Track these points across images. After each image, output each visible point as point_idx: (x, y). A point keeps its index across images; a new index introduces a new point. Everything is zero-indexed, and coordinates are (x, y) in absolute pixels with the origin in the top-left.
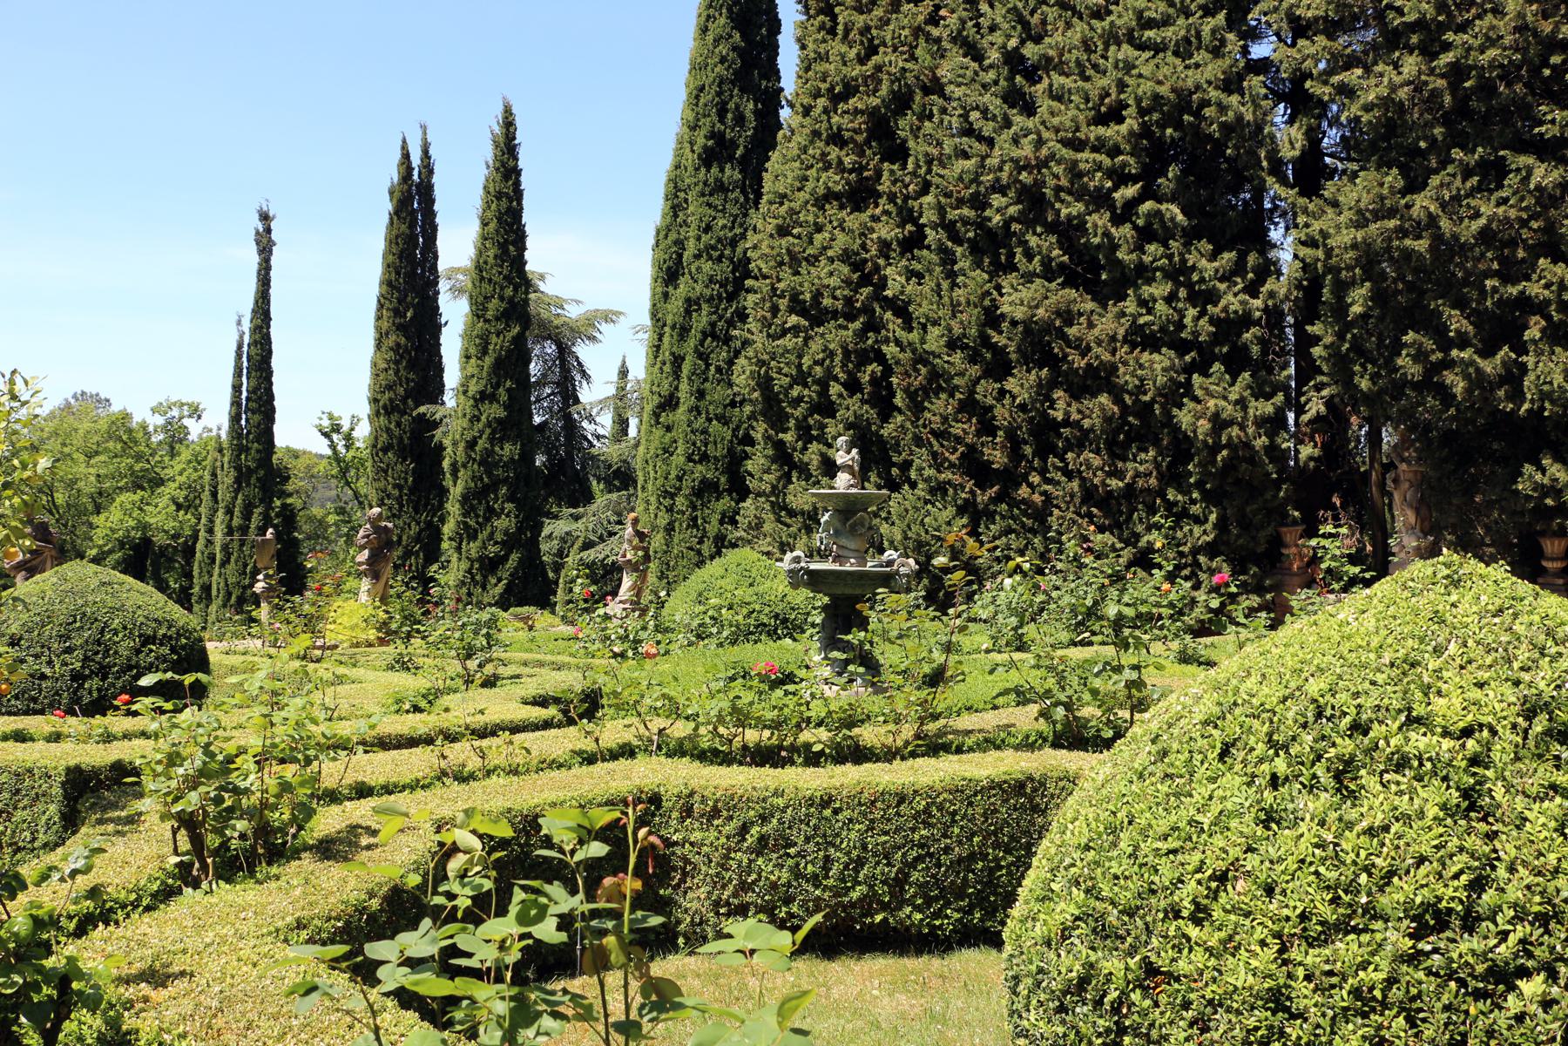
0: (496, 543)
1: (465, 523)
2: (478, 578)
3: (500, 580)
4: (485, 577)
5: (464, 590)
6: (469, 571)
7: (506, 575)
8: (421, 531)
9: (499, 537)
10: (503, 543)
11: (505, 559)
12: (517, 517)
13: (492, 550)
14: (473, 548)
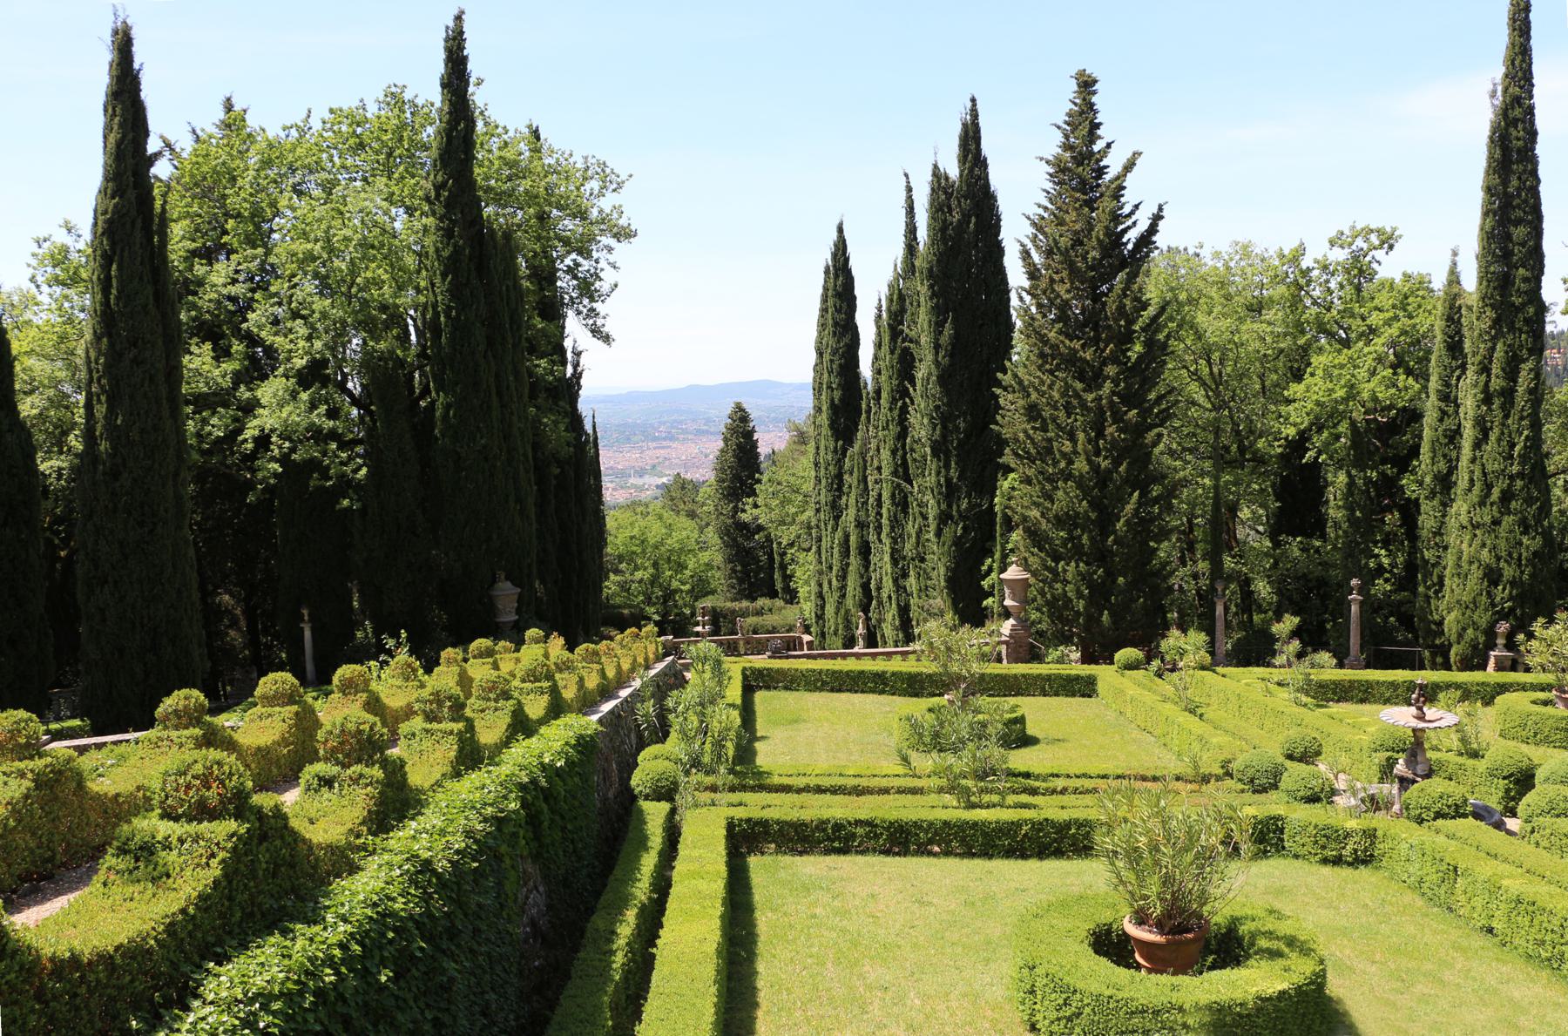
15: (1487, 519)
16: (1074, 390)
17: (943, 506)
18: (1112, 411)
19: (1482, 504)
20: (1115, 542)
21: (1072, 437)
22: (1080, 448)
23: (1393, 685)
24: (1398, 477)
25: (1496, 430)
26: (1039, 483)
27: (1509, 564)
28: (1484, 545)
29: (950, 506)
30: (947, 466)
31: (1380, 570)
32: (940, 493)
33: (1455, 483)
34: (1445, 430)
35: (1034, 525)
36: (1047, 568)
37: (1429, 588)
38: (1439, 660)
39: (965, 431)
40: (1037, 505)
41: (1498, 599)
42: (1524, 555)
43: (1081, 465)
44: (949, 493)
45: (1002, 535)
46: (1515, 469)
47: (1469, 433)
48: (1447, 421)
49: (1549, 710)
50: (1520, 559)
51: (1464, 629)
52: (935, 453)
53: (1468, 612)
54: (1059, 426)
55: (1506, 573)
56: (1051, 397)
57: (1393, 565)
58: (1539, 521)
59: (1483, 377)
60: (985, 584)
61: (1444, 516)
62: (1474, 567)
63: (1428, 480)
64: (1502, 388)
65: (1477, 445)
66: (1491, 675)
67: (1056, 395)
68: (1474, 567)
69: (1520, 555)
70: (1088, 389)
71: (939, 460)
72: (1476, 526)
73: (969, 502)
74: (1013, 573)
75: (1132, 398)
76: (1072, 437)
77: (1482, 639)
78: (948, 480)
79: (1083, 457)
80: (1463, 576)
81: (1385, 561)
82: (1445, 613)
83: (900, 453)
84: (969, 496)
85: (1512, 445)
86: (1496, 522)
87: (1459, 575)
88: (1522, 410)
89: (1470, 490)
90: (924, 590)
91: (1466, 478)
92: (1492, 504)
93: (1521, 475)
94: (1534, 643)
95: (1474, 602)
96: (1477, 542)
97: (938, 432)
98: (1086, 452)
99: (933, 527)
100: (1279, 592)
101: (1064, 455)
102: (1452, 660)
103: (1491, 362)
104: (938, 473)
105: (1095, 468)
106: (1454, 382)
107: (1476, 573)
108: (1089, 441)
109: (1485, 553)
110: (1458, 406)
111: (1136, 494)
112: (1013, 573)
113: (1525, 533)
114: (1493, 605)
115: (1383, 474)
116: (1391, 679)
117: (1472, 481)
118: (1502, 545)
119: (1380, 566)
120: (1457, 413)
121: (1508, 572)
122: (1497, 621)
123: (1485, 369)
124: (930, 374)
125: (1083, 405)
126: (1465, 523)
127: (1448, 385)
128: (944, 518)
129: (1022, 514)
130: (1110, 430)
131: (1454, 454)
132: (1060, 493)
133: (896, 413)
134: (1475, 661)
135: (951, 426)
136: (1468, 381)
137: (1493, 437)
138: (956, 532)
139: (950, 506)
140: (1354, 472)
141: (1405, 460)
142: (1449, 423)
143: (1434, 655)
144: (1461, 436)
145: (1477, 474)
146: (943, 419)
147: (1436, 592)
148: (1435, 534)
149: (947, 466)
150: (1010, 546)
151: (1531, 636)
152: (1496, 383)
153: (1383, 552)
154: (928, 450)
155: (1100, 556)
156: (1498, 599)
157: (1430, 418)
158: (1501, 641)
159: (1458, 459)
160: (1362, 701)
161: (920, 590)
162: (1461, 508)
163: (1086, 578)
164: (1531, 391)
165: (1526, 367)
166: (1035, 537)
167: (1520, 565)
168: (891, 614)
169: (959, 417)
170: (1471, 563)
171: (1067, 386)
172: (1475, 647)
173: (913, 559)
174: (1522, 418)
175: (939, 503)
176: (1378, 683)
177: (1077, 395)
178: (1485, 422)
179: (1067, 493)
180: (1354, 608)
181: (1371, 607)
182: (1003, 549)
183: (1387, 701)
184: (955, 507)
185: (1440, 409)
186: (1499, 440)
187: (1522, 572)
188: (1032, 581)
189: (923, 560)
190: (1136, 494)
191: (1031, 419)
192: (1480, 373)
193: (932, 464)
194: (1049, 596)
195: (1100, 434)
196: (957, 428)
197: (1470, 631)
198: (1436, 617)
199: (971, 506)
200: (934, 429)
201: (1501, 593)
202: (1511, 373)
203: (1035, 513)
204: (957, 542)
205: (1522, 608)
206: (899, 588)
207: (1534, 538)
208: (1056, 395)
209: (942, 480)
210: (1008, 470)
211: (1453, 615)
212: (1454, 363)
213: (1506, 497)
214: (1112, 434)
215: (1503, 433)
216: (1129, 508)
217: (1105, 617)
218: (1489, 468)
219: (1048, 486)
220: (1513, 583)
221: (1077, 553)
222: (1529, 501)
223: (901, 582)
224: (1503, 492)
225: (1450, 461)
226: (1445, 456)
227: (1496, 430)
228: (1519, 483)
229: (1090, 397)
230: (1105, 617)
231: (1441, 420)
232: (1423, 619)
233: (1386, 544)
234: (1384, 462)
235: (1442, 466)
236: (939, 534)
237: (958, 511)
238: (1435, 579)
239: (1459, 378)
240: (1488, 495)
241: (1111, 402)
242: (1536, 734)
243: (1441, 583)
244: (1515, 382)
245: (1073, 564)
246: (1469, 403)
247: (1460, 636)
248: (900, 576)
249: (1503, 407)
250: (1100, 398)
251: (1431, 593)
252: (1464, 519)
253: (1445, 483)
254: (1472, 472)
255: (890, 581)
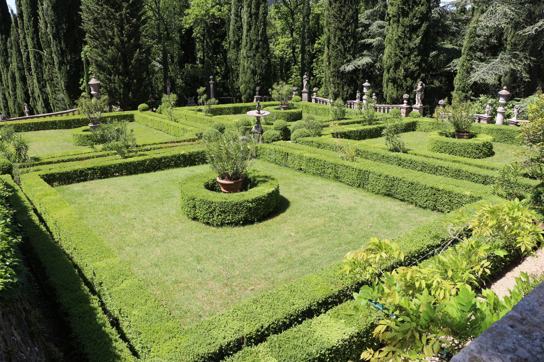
0: (417, 19)
1: (403, 8)
2: (408, 35)
3: (418, 36)
4: (411, 35)
5: (401, 41)
6: (404, 32)
7: (421, 34)
8: (354, 13)
9: (418, 15)
10: (420, 18)
11: (419, 26)
12: (426, 6)
13: (415, 22)
14: (406, 21)
15: (252, 55)
16: (111, 12)
17: (60, 59)
18: (127, 20)
19: (250, 50)
20: (132, 67)
21: (112, 29)
22: (115, 33)
23: (229, 108)
24: (221, 42)
25: (254, 26)
26: (101, 47)
27: (259, 69)
28: (251, 63)
29: (63, 58)
30: (60, 43)
31: (217, 73)
32: (58, 54)
33: (241, 44)
34: (237, 26)
35: (100, 63)
36: (107, 79)
37: (234, 78)
38: (238, 100)
39: (66, 29)
40: (101, 56)
41: (256, 80)
42: (263, 65)
43: (117, 40)
44: (62, 53)
45: (86, 68)
46: (260, 38)
47: (245, 27)
48: (237, 23)
49: (279, 111)
50: (262, 67)
51: (246, 90)
52: (54, 38)
53: (248, 84)
54: (106, 26)
55: (258, 71)
56: (102, 15)
57: (221, 71)
58: (267, 55)
59: (249, 9)
60: (81, 88)
61: (238, 54)
62: (249, 70)
63: (232, 43)
64: (255, 12)
65: (248, 31)
66: (255, 103)
67: (104, 13)
68: (249, 70)
69: (262, 65)
70: (117, 12)
71: (56, 40)
72: (248, 57)
73: (71, 57)
74: (93, 81)
75: (132, 15)
76: (112, 29)
77: (252, 92)
78: (61, 49)
79: (117, 37)
80: (245, 73)
81: (219, 70)
82: (240, 85)
83: (35, 39)
84: (70, 54)
85: (258, 31)
86: (255, 56)
87: (244, 73)
88: (261, 20)
89: (246, 46)
90: (54, 92)
91: (245, 41)
92: (253, 50)
93: (261, 40)
94: (274, 91)
95: (249, 81)
96: (249, 62)
97: (54, 30)
98: (118, 35)
99: (57, 67)
100: (185, 82)
101: (110, 36)
102: (243, 100)
103: (251, 4)
104: (57, 46)
105: (122, 41)
106: (239, 10)
107: (249, 71)
108: (119, 31)
109: (252, 66)
110: (241, 18)
111: (138, 50)
112: (93, 81)
113: (263, 59)
114: (255, 82)
115: (216, 42)
116: (228, 107)
117: (247, 42)
118: (257, 63)
119: (217, 72)
120: (241, 21)
121: (259, 71)
122: (256, 87)
123: (249, 6)
124: (48, 6)
125: (115, 18)
126: (245, 56)
127: (237, 11)
128: (61, 63)
129: (95, 59)
130: (126, 27)
131: (240, 34)
132: (110, 51)
133: (31, 23)
134: (250, 99)
135: (59, 27)
136: (245, 10)
137: (253, 28)
138: (67, 68)
139: (63, 58)
140: (208, 40)
141: (223, 36)
142: (239, 24)
143: (236, 99)
144: (243, 29)
145: (248, 40)
146: (57, 25)
147: (236, 79)
148: (235, 60)
149: (60, 43)
150: (89, 72)
151: (273, 89)
152: (253, 11)
153: (217, 67)
154: (51, 36)
155: (126, 73)
156: (256, 80)
157: (232, 22)
158: (257, 93)
159: (242, 35)
160: (220, 114)
161: (52, 92)
162: (243, 52)
163: (121, 81)
164: (263, 14)
165: (262, 5)
166: (100, 67)
167: (262, 69)
168: (40, 103)
169: (63, 23)
170: (248, 69)
171: (108, 11)
172: (249, 95)
173: (48, 80)
174: (261, 22)
175: (58, 58)
176: (224, 108)
177: (112, 14)
178: (250, 23)
179: (112, 51)
180: (211, 86)
181: (216, 85)
182: (87, 74)
183: (228, 114)
184: (65, 59)
185: (235, 19)
186: (254, 29)
187: (263, 71)
188: (101, 84)
189: (52, 80)
190: (138, 50)
191: (95, 23)
192: (248, 7)
193: (53, 43)
194: (109, 89)
195: (123, 28)
196: (63, 28)
197: (248, 90)
198: (237, 87)
199: (71, 58)
200: (53, 28)
201: (257, 78)
202: (258, 8)
203: (100, 59)
204: (68, 72)
205: (263, 82)
206: (42, 92)
207: (265, 60)
208: (104, 13)
209: (59, 49)
210: (86, 43)
211: (243, 86)
212: (239, 4)
213: (257, 47)
214: (127, 28)
215: (255, 27)
216: (136, 55)
217: (130, 95)
218: (252, 38)
219: (104, 48)
220: (260, 74)
221: (118, 73)
222: (264, 49)
223: (44, 90)
224: (256, 46)
225: (239, 36)
226: (237, 35)
227: (254, 26)
228: (261, 43)
229: (118, 14)
230: (130, 95)
231: (236, 23)
232: (232, 87)
233: (218, 65)
234: (216, 37)
235: (237, 38)
236: (60, 69)
237: (67, 60)
238: (236, 75)
239: (241, 9)
240: (252, 47)
241: (126, 16)
242: (277, 118)
243: (238, 76)
244: (259, 10)
245: (117, 76)
246: (245, 17)
247: (245, 93)
248: (42, 88)
249: (255, 19)
250: (121, 15)
251: (235, 79)
252: (245, 55)
253: (238, 44)
254: (247, 40)
255: (38, 90)
